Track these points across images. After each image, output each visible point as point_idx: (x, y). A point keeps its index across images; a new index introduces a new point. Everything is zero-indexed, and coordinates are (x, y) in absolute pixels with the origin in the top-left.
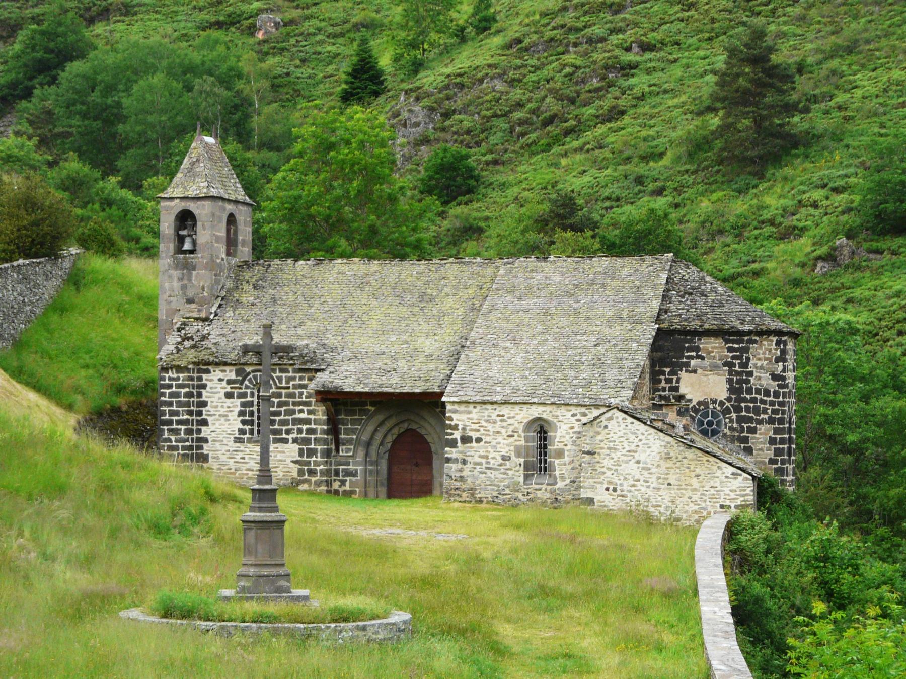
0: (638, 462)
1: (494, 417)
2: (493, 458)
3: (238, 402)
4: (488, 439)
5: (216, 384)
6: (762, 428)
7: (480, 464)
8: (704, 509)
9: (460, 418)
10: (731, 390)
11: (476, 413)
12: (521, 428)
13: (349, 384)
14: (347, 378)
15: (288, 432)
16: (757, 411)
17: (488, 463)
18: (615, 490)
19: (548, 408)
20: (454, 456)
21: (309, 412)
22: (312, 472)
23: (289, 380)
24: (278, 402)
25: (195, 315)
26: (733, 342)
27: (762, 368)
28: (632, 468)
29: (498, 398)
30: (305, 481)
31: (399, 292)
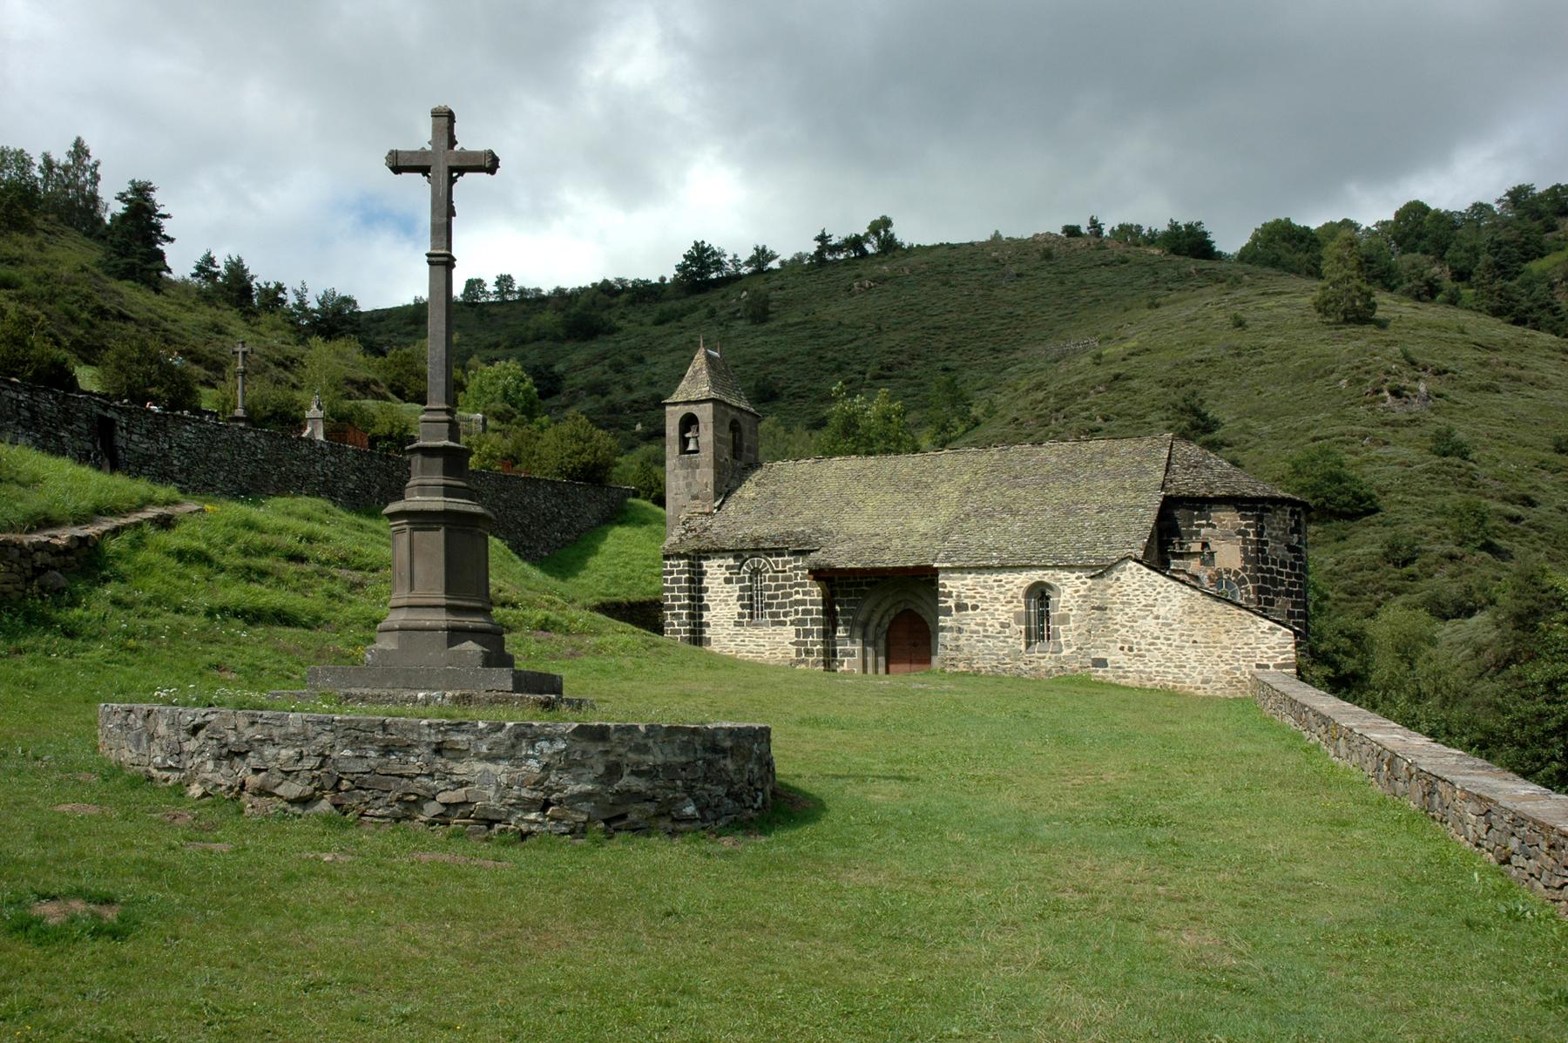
0: (1157, 617)
1: (990, 582)
3: (737, 587)
4: (985, 606)
5: (715, 570)
6: (1280, 600)
7: (977, 632)
8: (1238, 669)
9: (953, 586)
10: (1246, 559)
11: (970, 579)
12: (1021, 592)
13: (842, 563)
14: (841, 557)
15: (786, 615)
16: (1274, 582)
18: (1131, 649)
19: (1050, 572)
20: (949, 624)
21: (805, 593)
22: (808, 652)
23: (785, 563)
26: (1247, 509)
27: (1276, 538)
29: (996, 562)
30: (803, 661)
31: (895, 483)
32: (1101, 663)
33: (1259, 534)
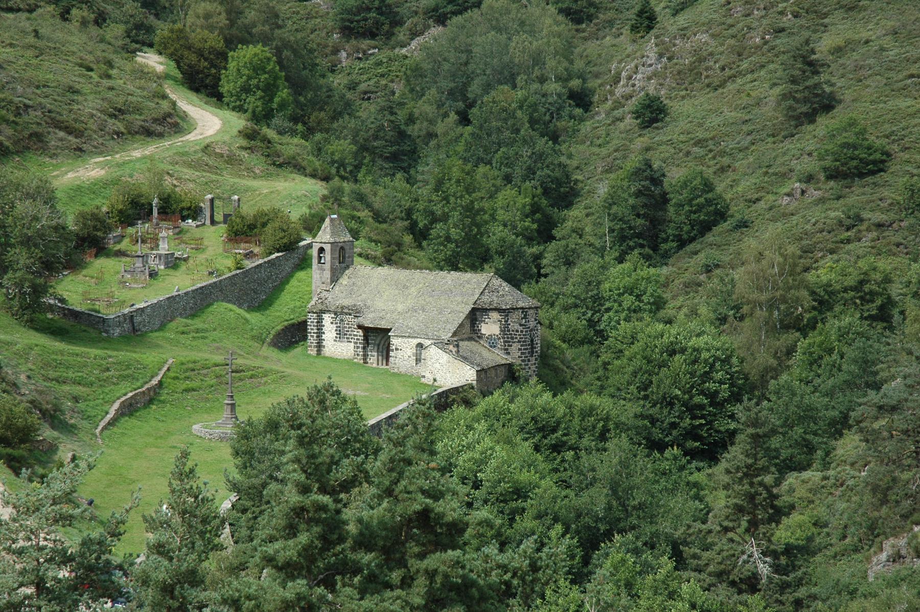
5: (327, 318)
10: (501, 331)
16: (512, 338)
28: (437, 365)
32: (424, 377)
33: (506, 321)
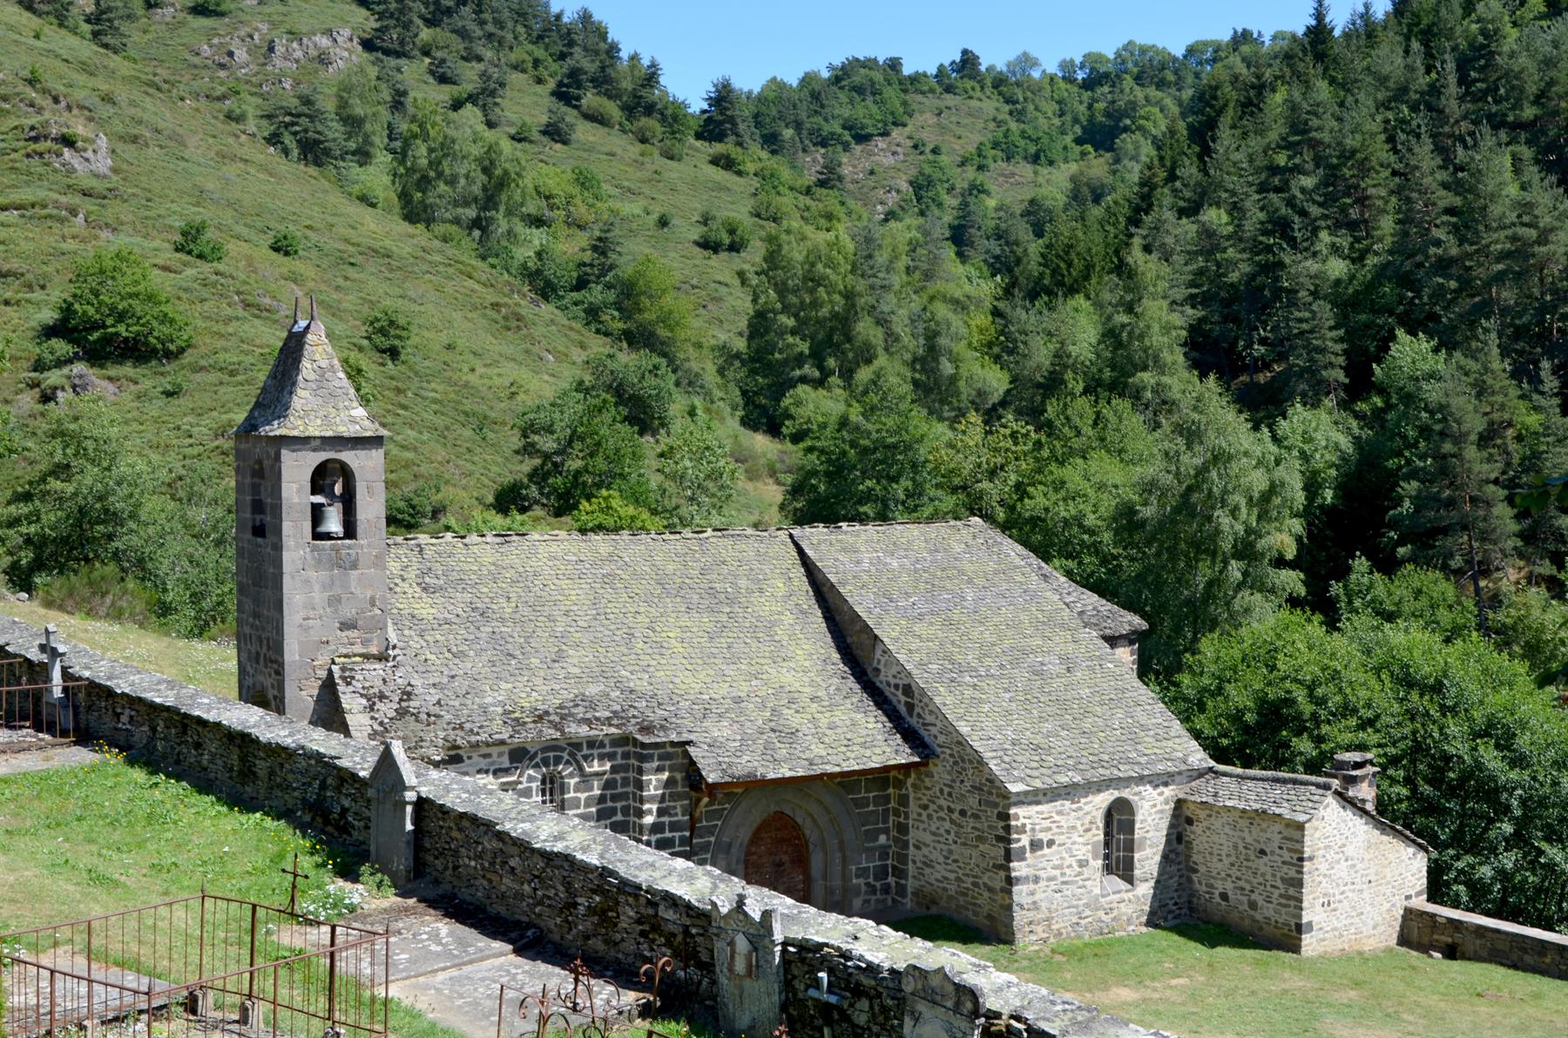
2: (1070, 866)
17: (1063, 874)
24: (587, 799)
25: (359, 649)
